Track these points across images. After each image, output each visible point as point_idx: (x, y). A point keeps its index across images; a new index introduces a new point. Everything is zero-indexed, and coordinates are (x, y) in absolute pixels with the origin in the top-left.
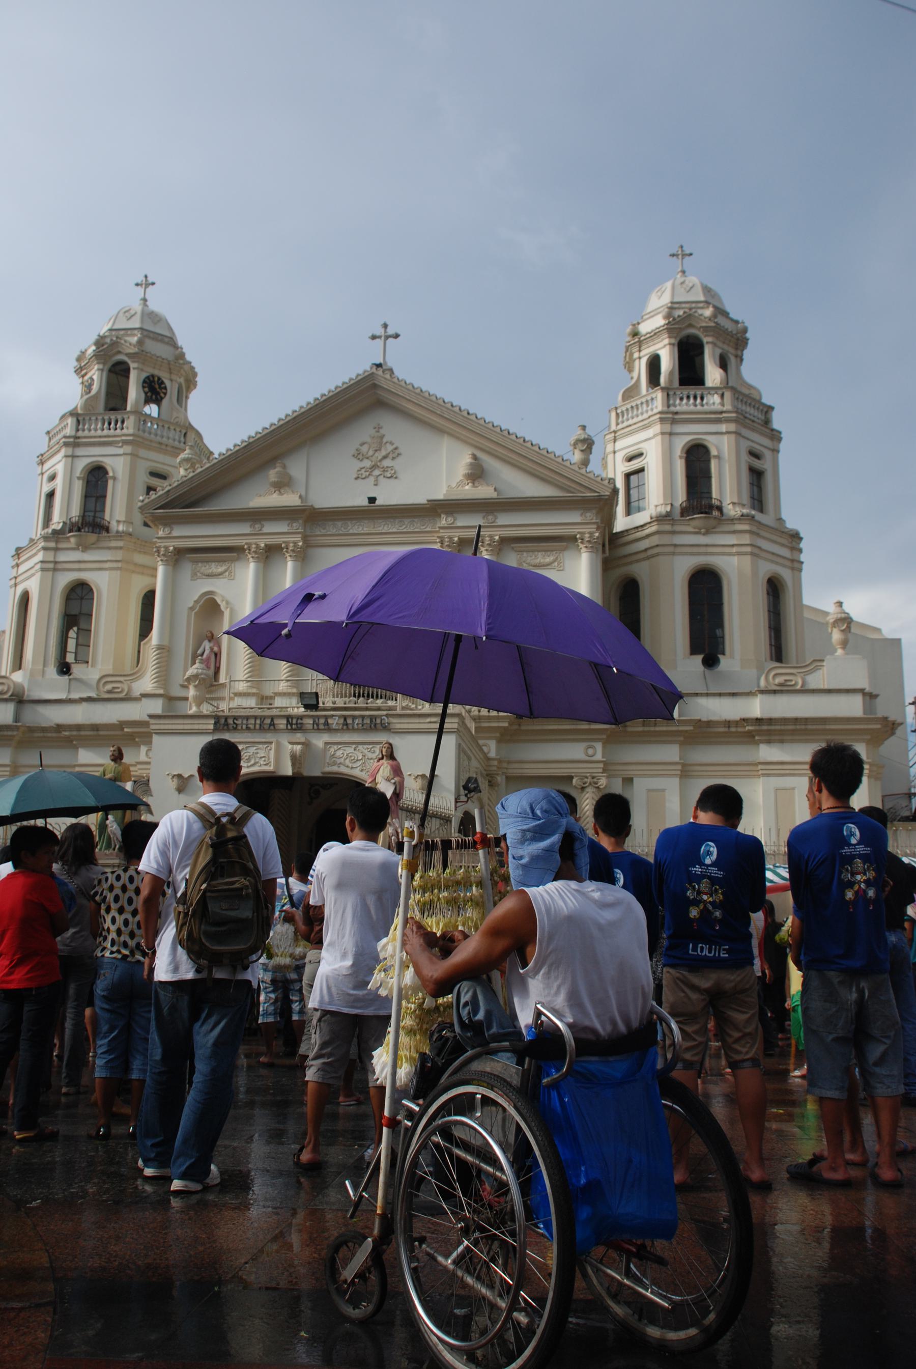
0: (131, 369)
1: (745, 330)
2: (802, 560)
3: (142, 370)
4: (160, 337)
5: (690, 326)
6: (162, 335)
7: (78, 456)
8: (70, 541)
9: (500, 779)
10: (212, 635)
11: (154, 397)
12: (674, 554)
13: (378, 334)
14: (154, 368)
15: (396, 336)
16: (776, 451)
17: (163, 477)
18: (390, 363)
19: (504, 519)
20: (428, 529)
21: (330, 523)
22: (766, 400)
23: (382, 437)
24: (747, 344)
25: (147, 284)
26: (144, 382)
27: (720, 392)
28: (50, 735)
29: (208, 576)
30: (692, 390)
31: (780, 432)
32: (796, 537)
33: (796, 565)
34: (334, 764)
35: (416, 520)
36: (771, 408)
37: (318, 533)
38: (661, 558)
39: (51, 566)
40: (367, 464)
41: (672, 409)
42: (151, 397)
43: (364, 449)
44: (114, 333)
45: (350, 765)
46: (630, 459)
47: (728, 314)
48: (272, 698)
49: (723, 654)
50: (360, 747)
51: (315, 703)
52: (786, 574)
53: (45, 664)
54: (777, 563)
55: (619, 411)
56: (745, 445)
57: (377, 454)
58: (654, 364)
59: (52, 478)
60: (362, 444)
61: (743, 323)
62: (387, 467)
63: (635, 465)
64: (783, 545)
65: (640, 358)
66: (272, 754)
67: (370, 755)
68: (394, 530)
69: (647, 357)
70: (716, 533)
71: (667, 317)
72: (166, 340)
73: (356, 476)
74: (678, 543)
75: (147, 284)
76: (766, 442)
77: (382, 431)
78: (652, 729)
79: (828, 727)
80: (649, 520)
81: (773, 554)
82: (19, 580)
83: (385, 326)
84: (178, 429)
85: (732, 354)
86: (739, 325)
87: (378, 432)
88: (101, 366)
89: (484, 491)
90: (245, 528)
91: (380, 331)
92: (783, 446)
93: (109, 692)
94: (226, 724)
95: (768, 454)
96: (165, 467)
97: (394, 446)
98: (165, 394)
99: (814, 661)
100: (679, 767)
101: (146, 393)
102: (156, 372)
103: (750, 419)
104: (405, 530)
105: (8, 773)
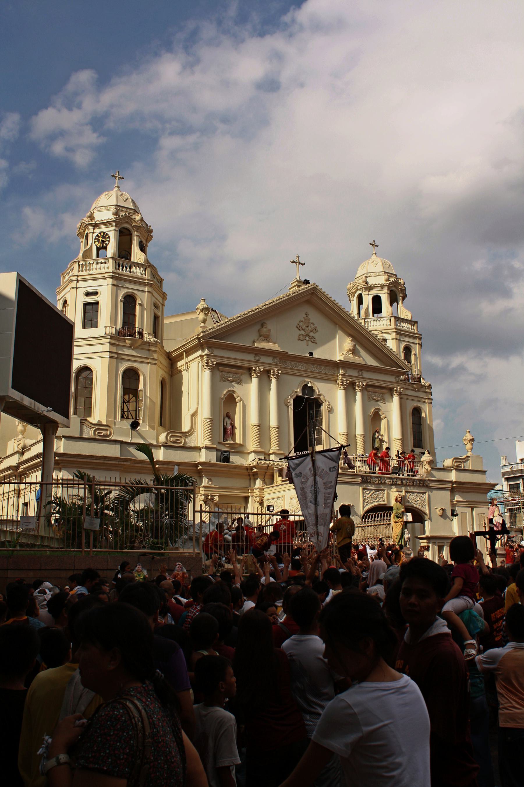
8: (125, 342)
12: (407, 399)
13: (296, 261)
15: (303, 264)
19: (366, 375)
21: (289, 362)
23: (309, 320)
28: (145, 466)
35: (327, 368)
37: (283, 366)
39: (116, 356)
40: (303, 332)
53: (115, 418)
57: (307, 329)
58: (377, 301)
60: (300, 322)
65: (368, 295)
66: (385, 495)
69: (372, 296)
71: (388, 280)
87: (307, 317)
88: (117, 229)
89: (358, 360)
91: (297, 260)
93: (173, 442)
104: (322, 372)
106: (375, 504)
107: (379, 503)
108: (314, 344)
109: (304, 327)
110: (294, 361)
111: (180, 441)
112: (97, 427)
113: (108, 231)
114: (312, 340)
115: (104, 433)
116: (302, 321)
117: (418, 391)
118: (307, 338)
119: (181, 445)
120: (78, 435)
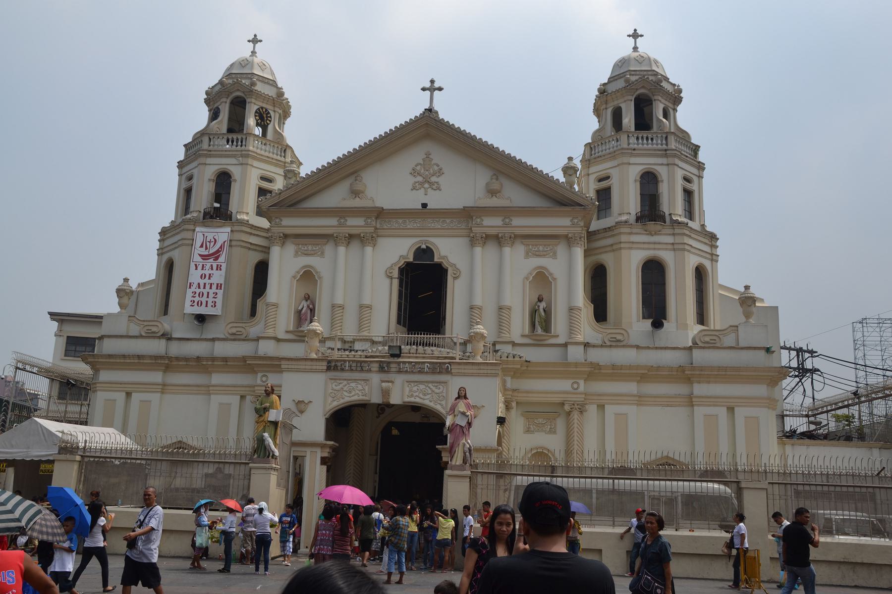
0: (247, 103)
1: (680, 91)
2: (718, 254)
3: (255, 104)
4: (266, 81)
5: (643, 87)
6: (268, 79)
7: (210, 164)
9: (514, 404)
10: (309, 296)
11: (263, 123)
12: (631, 248)
14: (263, 102)
15: (440, 89)
16: (700, 177)
17: (269, 180)
18: (436, 107)
19: (517, 221)
20: (463, 227)
21: (394, 220)
22: (694, 141)
24: (681, 101)
25: (255, 41)
26: (256, 112)
27: (664, 136)
29: (305, 254)
30: (644, 134)
31: (704, 164)
32: (713, 237)
33: (714, 257)
34: (412, 396)
36: (699, 147)
37: (386, 227)
38: (623, 251)
40: (420, 179)
41: (631, 146)
42: (261, 123)
43: (418, 168)
44: (234, 76)
45: (422, 397)
46: (600, 180)
47: (669, 79)
48: (353, 342)
49: (665, 319)
50: (430, 385)
51: (399, 353)
52: (707, 264)
54: (702, 256)
55: (592, 146)
56: (679, 174)
57: (427, 173)
59: (190, 178)
60: (416, 166)
61: (678, 86)
62: (435, 182)
63: (604, 184)
64: (705, 243)
65: (606, 109)
66: (367, 388)
67: (437, 391)
68: (439, 227)
69: (611, 108)
70: (661, 234)
71: (627, 81)
72: (271, 82)
73: (411, 187)
74: (634, 241)
75: (255, 41)
76: (695, 171)
77: (430, 156)
78: (619, 371)
79: (741, 373)
80: (614, 224)
81: (700, 250)
82: (165, 250)
83: (432, 82)
84: (280, 147)
85: (671, 108)
86: (676, 88)
88: (224, 100)
90: (333, 221)
91: (428, 85)
92: (706, 173)
94: (336, 366)
95: (695, 179)
96: (271, 174)
97: (439, 167)
98: (270, 121)
99: (731, 326)
100: (637, 398)
101: (257, 121)
102: (264, 105)
103: (685, 155)
104: (447, 227)
105: (160, 390)
106: (347, 399)
107: (356, 398)
108: (438, 190)
109: (422, 171)
110: (402, 218)
111: (241, 333)
112: (146, 323)
113: (219, 105)
114: (434, 187)
115: (154, 329)
116: (420, 164)
117: (656, 234)
118: (426, 185)
119: (242, 337)
120: (125, 334)
